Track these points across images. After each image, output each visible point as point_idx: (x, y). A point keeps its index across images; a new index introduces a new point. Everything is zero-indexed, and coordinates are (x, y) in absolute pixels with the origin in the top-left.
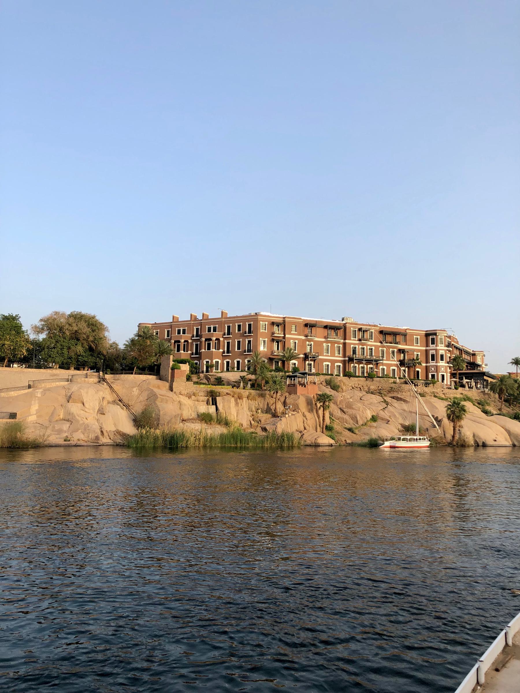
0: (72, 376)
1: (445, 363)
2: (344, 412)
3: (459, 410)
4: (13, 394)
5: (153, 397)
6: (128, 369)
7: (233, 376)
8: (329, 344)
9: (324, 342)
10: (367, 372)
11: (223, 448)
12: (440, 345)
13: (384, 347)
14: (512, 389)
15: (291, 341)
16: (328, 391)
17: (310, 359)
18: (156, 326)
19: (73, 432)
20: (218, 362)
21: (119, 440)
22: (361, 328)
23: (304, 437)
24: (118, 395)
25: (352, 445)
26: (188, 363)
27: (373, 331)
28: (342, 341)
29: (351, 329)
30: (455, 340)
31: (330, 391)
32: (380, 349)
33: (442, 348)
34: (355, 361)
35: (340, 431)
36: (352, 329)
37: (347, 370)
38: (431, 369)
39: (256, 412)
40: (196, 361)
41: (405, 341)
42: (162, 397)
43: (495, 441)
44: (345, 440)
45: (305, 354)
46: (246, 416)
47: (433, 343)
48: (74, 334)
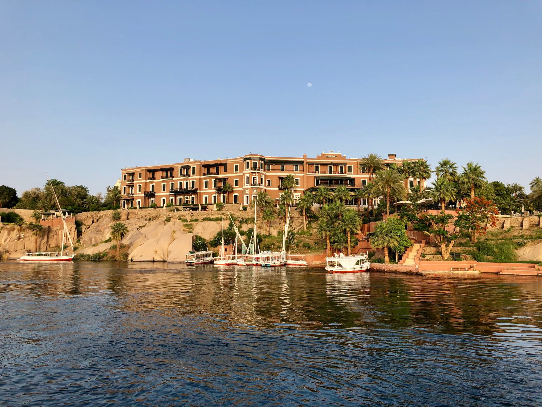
12: (246, 169)
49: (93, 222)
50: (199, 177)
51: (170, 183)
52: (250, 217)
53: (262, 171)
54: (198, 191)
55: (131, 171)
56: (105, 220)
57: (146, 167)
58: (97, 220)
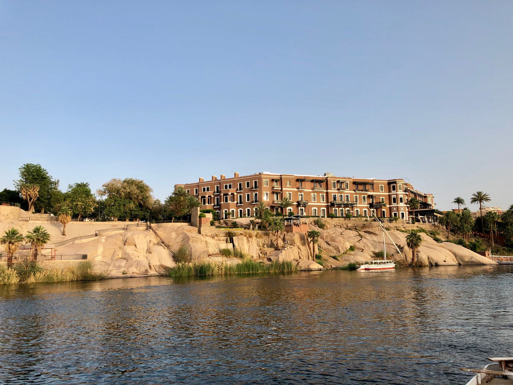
0: (127, 226)
1: (404, 204)
2: (329, 244)
3: (416, 239)
4: (84, 241)
5: (186, 239)
6: (168, 219)
7: (245, 221)
8: (316, 194)
9: (312, 192)
10: (345, 213)
11: (239, 275)
12: (399, 191)
13: (357, 194)
14: (456, 222)
15: (287, 192)
16: (316, 229)
17: (301, 205)
18: (187, 186)
19: (129, 267)
20: (234, 210)
21: (162, 271)
22: (339, 181)
23: (300, 264)
24: (161, 239)
25: (336, 269)
26: (211, 213)
27: (348, 182)
28: (325, 191)
29: (331, 182)
30: (411, 187)
31: (318, 229)
32: (354, 195)
33: (401, 193)
34: (335, 206)
35: (327, 259)
36: (332, 181)
37: (330, 213)
38: (394, 209)
39: (263, 247)
40: (217, 211)
41: (373, 189)
42: (193, 238)
43: (445, 261)
44: (331, 266)
45: (298, 202)
46: (255, 250)
47: (394, 189)
48: (127, 195)
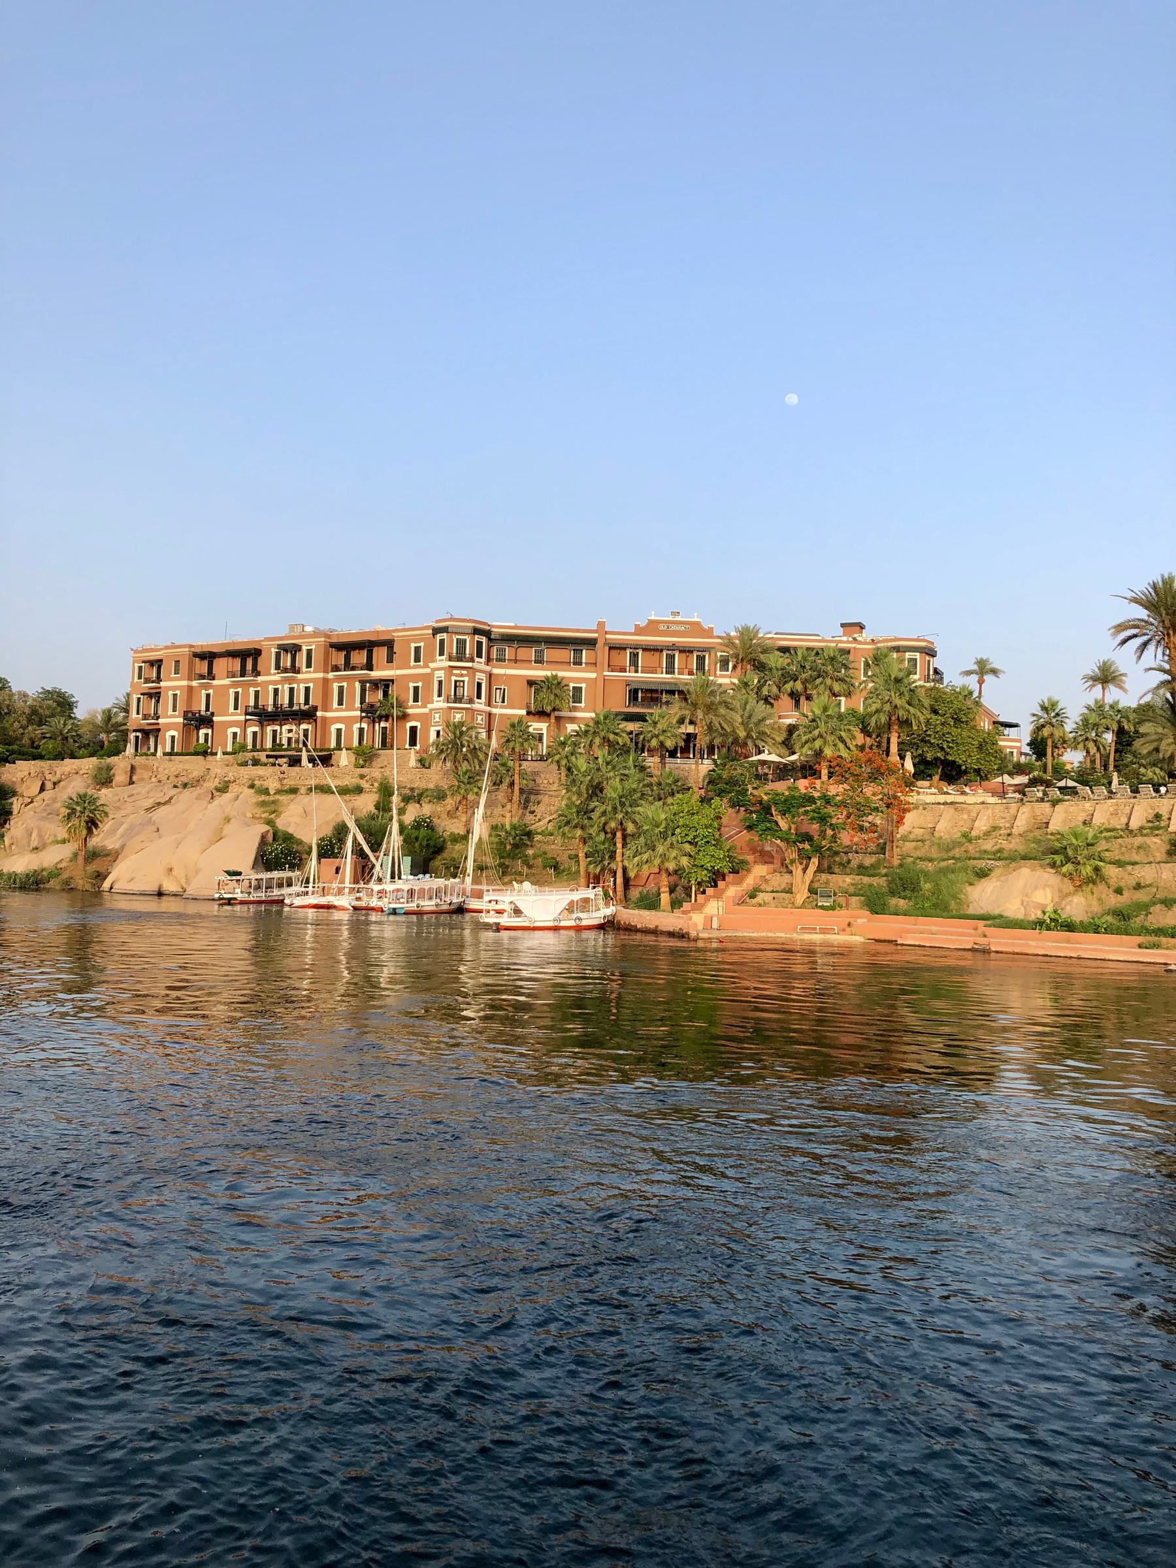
12: (438, 658)
49: (42, 789)
50: (321, 675)
51: (252, 690)
52: (431, 786)
53: (480, 663)
54: (319, 714)
55: (154, 656)
56: (73, 784)
57: (191, 646)
58: (55, 784)
